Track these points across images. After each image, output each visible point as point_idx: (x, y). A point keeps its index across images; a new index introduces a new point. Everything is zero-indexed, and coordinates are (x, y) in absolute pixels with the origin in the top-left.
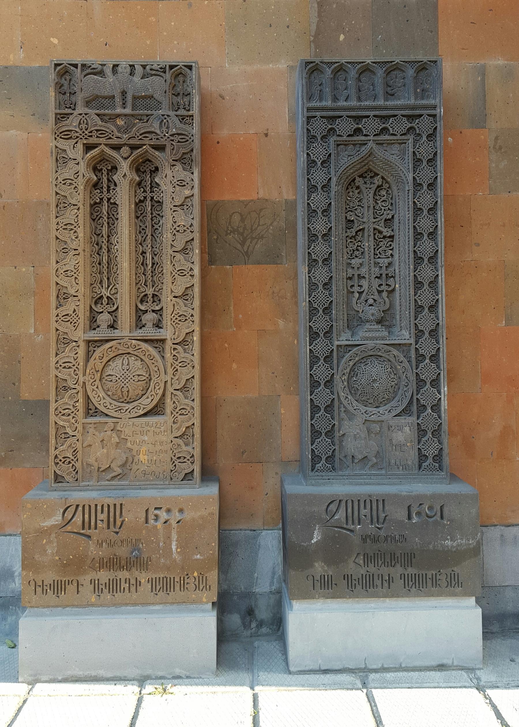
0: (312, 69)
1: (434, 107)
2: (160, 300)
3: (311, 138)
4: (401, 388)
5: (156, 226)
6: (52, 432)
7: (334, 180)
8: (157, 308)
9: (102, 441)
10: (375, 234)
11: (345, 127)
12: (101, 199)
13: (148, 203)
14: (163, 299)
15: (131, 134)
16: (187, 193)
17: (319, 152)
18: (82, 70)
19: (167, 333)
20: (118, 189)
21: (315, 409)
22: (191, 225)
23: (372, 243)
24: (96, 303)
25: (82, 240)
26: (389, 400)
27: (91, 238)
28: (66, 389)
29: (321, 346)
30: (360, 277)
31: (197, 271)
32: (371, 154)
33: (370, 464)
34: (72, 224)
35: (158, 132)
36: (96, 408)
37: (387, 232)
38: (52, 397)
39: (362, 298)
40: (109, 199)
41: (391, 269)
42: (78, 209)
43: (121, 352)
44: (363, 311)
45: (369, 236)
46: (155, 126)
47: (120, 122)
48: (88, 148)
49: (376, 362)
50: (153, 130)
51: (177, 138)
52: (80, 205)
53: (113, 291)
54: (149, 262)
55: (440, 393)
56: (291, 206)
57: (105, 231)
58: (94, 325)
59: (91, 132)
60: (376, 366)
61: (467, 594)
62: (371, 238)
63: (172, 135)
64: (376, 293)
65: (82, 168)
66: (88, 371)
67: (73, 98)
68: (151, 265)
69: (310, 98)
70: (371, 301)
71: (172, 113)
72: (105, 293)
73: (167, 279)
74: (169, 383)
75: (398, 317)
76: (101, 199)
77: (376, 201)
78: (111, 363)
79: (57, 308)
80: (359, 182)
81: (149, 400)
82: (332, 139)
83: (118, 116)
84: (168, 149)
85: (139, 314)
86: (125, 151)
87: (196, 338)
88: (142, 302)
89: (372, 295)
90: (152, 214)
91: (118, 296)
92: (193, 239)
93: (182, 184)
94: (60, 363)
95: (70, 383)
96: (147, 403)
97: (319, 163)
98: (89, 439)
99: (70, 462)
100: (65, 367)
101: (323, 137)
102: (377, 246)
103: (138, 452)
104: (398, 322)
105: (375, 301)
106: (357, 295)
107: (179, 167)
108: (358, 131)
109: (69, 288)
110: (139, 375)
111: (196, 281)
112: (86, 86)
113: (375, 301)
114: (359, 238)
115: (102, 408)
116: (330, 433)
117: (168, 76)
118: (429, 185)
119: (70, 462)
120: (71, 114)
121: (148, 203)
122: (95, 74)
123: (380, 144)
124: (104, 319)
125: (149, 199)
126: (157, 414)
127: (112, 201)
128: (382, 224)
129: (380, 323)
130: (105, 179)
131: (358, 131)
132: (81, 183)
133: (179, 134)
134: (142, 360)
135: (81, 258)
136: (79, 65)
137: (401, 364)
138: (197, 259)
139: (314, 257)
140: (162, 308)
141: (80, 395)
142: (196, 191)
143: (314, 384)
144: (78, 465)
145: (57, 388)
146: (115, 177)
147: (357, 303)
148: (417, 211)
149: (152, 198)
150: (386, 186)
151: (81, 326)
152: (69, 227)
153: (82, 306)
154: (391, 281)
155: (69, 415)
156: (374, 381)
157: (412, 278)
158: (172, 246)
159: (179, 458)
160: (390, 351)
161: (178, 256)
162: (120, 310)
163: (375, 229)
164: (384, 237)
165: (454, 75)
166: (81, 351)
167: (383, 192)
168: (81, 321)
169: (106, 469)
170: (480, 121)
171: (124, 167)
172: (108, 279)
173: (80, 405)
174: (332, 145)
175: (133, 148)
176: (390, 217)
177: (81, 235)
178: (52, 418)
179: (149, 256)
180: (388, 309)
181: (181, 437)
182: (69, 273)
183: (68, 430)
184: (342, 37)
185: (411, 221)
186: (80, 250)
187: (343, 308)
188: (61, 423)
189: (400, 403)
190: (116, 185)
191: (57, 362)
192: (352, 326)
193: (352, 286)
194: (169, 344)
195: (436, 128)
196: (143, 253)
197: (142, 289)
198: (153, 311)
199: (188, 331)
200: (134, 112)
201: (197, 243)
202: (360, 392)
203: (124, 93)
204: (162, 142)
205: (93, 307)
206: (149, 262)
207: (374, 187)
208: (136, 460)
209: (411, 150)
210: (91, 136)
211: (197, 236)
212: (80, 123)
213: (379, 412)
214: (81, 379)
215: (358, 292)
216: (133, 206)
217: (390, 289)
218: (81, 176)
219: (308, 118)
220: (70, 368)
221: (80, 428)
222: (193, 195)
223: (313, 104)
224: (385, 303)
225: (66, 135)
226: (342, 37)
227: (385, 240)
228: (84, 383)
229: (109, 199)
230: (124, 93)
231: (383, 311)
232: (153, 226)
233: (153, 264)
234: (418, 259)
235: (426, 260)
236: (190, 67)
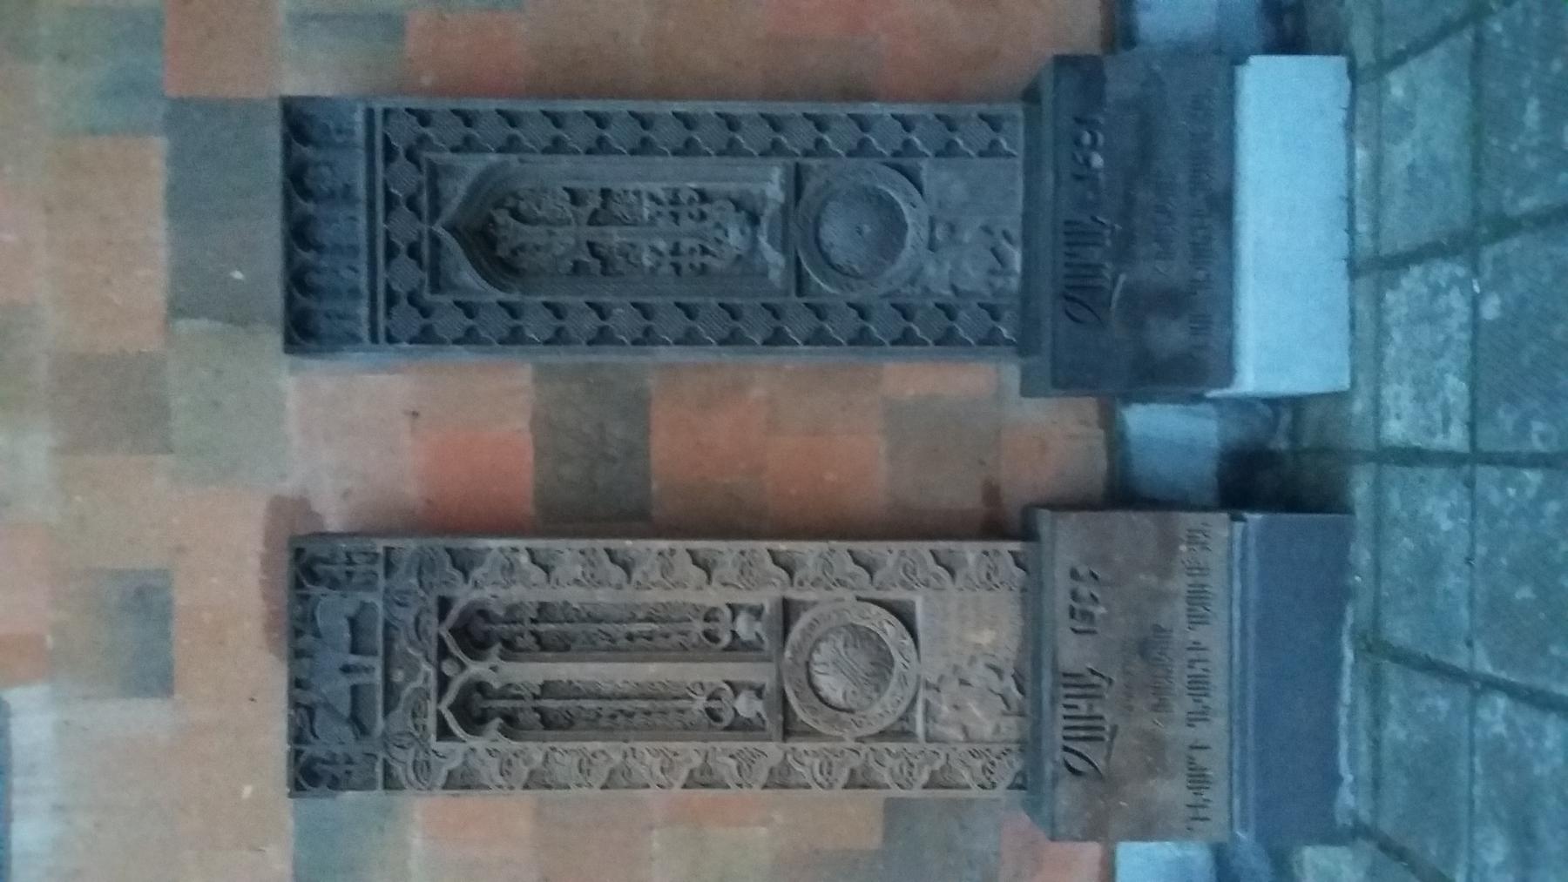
0: (302, 333)
1: (370, 113)
2: (714, 609)
3: (426, 337)
5: (584, 615)
6: (940, 793)
7: (502, 296)
8: (728, 613)
9: (956, 707)
10: (599, 224)
11: (407, 275)
12: (536, 709)
13: (542, 628)
14: (710, 603)
15: (419, 655)
16: (524, 559)
17: (450, 321)
18: (307, 743)
19: (767, 598)
20: (517, 680)
21: (906, 339)
22: (582, 552)
23: (613, 230)
24: (717, 719)
25: (610, 744)
26: (892, 206)
27: (605, 729)
28: (867, 770)
29: (798, 324)
30: (676, 251)
31: (664, 544)
32: (452, 229)
33: (1004, 243)
34: (581, 762)
35: (414, 611)
36: (901, 719)
37: (595, 202)
38: (883, 793)
40: (535, 697)
41: (661, 195)
42: (553, 749)
43: (803, 677)
45: (603, 234)
46: (406, 616)
47: (398, 676)
48: (444, 733)
50: (412, 620)
51: (426, 579)
52: (547, 746)
53: (699, 691)
54: (646, 627)
55: (881, 116)
56: (544, 374)
57: (591, 704)
58: (757, 721)
59: (416, 727)
61: (1231, 82)
62: (605, 229)
63: (421, 583)
65: (478, 743)
66: (837, 733)
67: (357, 759)
68: (653, 626)
69: (354, 339)
70: (719, 234)
71: (382, 582)
72: (700, 703)
73: (676, 596)
74: (863, 595)
75: (747, 185)
76: (536, 709)
77: (537, 221)
78: (822, 694)
79: (728, 787)
80: (503, 251)
81: (887, 627)
82: (427, 296)
83: (387, 676)
84: (445, 592)
85: (738, 648)
86: (448, 668)
87: (782, 546)
88: (716, 640)
90: (560, 622)
91: (706, 681)
92: (608, 551)
93: (510, 568)
94: (820, 779)
95: (856, 762)
96: (891, 630)
97: (470, 322)
98: (954, 733)
99: (993, 764)
100: (829, 773)
101: (425, 312)
102: (621, 221)
103: (978, 646)
106: (707, 259)
107: (477, 573)
108: (413, 251)
109: (692, 766)
110: (845, 646)
111: (680, 545)
112: (334, 738)
114: (604, 252)
115: (901, 709)
116: (949, 312)
117: (316, 591)
118: (513, 125)
119: (993, 764)
120: (385, 761)
121: (542, 628)
122: (312, 720)
123: (435, 212)
124: (746, 706)
125: (534, 627)
126: (913, 615)
127: (538, 692)
128: (580, 210)
130: (502, 704)
131: (413, 251)
132: (506, 745)
133: (420, 573)
134: (819, 640)
135: (640, 746)
136: (298, 747)
138: (642, 544)
139: (639, 335)
140: (730, 606)
141: (876, 745)
142: (521, 543)
143: (861, 339)
144: (997, 749)
145: (864, 786)
146: (497, 685)
148: (556, 146)
149: (533, 621)
150: (511, 202)
151: (757, 745)
152: (585, 766)
153: (725, 744)
154: (683, 198)
155: (911, 765)
156: (860, 232)
157: (679, 160)
158: (619, 587)
159: (988, 576)
161: (637, 576)
162: (731, 679)
163: (590, 223)
164: (604, 205)
165: (309, 74)
166: (803, 746)
167: (523, 206)
168: (750, 745)
169: (1006, 702)
170: (392, 25)
171: (476, 669)
172: (676, 698)
173: (894, 747)
174: (439, 298)
175: (443, 653)
176: (567, 196)
177: (599, 745)
178: (916, 793)
179: (635, 628)
181: (952, 572)
182: (666, 766)
183: (937, 766)
184: (238, 275)
185: (575, 158)
186: (626, 746)
188: (925, 777)
190: (510, 685)
191: (820, 785)
193: (692, 266)
194: (793, 594)
195: (408, 110)
196: (630, 637)
197: (695, 640)
198: (734, 618)
199: (768, 559)
200: (381, 652)
201: (614, 544)
203: (346, 669)
204: (432, 603)
205: (726, 723)
206: (646, 627)
207: (512, 221)
208: (991, 652)
209: (448, 156)
210: (424, 727)
211: (600, 544)
212: (401, 747)
214: (852, 744)
216: (549, 655)
217: (696, 197)
218: (496, 746)
219: (391, 339)
220: (830, 764)
221: (932, 747)
222: (529, 550)
223: (364, 331)
225: (422, 769)
226: (238, 275)
227: (606, 208)
228: (860, 740)
229: (535, 697)
230: (346, 669)
232: (584, 621)
233: (649, 620)
234: (644, 147)
235: (646, 133)
236: (299, 552)
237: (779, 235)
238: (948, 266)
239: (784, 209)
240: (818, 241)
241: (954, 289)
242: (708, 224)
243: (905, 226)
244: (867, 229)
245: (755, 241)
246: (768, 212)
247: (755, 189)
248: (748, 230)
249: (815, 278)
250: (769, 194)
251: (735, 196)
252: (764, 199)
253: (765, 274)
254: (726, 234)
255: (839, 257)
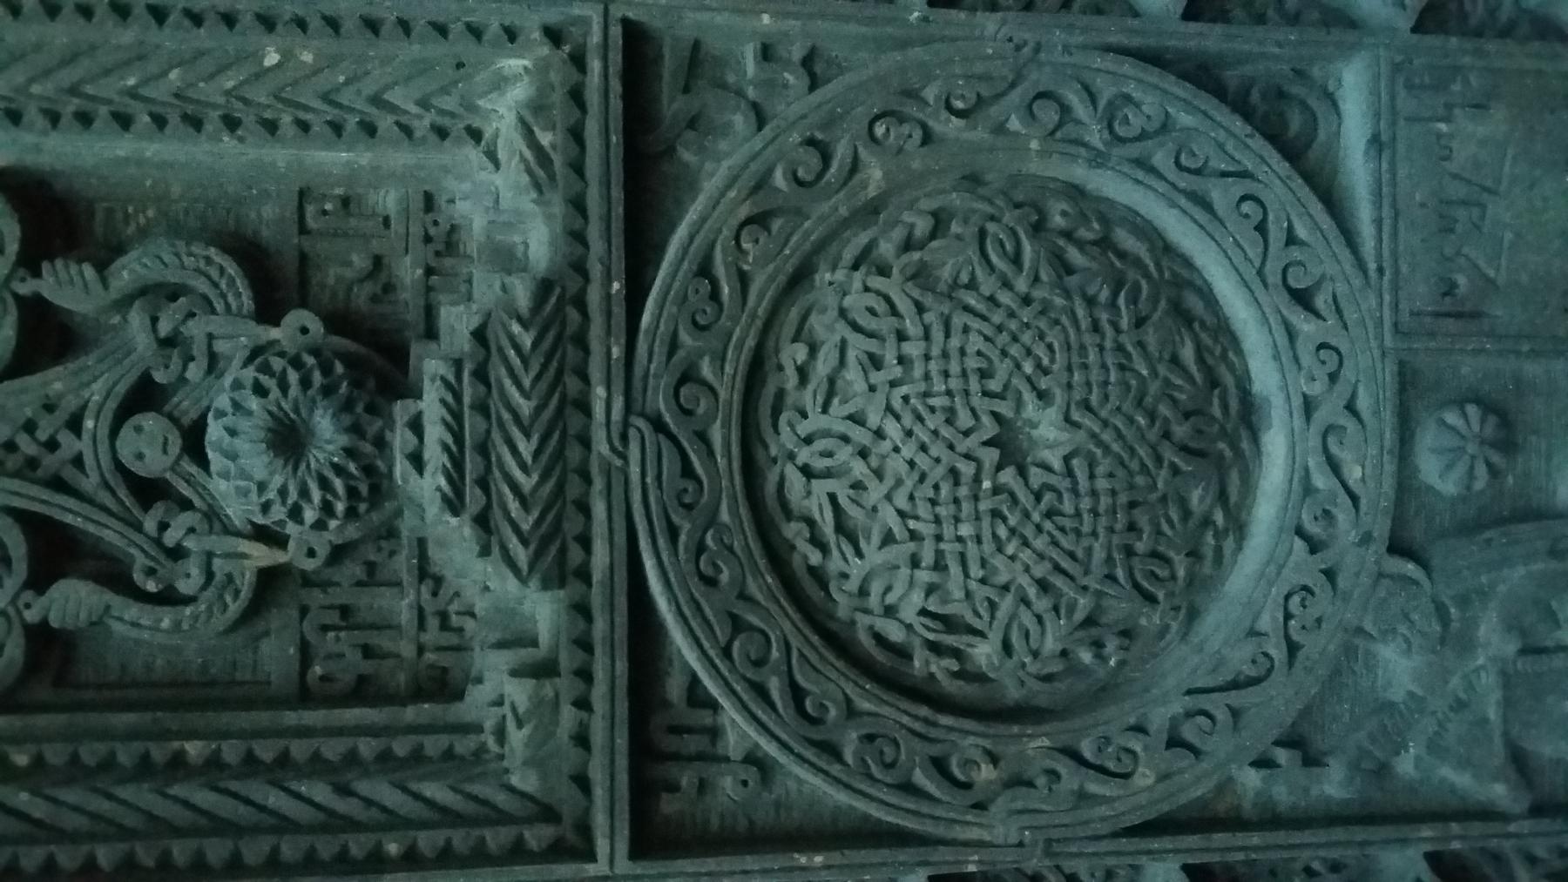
4: (1078, 172)
26: (1181, 298)
39: (111, 535)
44: (263, 535)
49: (815, 422)
60: (857, 419)
64: (55, 381)
70: (149, 445)
75: (333, 160)
89: (75, 424)
104: (400, 158)
105: (144, 396)
106: (72, 600)
113: (144, 396)
129: (398, 355)
137: (841, 152)
147: (168, 598)
156: (1009, 446)
160: (704, 270)
180: (250, 254)
187: (214, 763)
189: (1221, 195)
192: (432, 635)
202: (1119, 607)
213: (1309, 406)
215: (39, 581)
224: (174, 293)
231: (268, 312)
237: (519, 458)
238: (1493, 638)
239: (558, 298)
240: (765, 513)
241: (1520, 762)
242: (92, 384)
243: (1249, 414)
244: (1047, 430)
245: (371, 486)
246: (457, 321)
247: (382, 172)
248: (325, 426)
249: (738, 730)
250: (473, 217)
251: (269, 218)
252: (446, 244)
253: (443, 686)
254: (194, 441)
255: (886, 589)
